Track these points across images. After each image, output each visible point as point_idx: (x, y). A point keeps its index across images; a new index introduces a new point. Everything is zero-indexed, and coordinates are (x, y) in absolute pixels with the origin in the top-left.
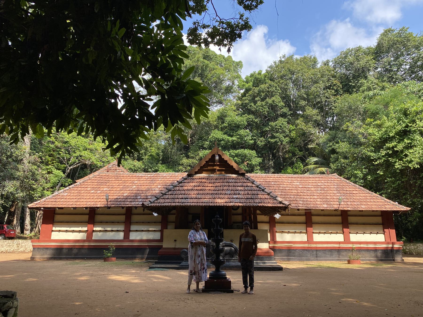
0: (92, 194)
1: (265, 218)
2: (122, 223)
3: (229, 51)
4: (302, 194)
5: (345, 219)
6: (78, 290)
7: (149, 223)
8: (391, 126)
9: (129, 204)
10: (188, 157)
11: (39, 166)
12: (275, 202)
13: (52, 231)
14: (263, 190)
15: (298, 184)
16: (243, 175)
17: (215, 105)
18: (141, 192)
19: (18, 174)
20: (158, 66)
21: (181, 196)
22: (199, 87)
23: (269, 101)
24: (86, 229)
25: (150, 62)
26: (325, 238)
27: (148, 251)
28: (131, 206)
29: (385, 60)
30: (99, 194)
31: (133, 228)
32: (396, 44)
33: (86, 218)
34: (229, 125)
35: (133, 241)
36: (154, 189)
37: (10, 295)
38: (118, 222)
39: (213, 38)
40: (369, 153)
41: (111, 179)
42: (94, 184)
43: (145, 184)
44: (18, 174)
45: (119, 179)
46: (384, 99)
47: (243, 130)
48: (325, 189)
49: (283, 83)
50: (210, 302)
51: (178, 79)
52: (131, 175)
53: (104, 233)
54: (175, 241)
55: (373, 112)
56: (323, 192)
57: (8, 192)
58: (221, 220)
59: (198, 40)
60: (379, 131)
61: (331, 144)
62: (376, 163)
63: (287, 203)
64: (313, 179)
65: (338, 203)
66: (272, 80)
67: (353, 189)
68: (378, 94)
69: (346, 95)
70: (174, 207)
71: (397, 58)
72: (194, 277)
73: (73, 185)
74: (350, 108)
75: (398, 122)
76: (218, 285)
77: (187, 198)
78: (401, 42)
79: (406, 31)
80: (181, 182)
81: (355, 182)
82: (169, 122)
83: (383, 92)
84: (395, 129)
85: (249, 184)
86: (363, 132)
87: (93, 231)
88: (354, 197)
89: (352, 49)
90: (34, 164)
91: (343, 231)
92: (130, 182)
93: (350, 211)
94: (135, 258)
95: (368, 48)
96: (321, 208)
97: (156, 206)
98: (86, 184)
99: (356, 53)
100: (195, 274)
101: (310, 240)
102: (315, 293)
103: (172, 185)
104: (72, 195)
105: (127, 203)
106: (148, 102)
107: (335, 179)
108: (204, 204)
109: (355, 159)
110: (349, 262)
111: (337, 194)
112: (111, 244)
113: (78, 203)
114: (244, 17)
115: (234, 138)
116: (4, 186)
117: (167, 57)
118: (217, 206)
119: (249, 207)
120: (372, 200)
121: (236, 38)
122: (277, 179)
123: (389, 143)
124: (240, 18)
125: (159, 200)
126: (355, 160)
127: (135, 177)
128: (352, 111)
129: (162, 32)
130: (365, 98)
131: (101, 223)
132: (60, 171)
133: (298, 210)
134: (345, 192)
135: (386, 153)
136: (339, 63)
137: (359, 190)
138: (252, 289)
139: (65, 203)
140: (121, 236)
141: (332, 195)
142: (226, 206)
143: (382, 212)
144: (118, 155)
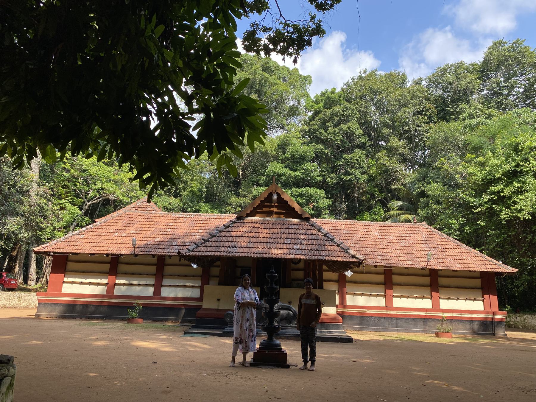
0: (116, 238)
1: (334, 276)
2: (152, 275)
3: (295, 61)
4: (380, 247)
5: (434, 281)
6: (93, 357)
7: (186, 276)
8: (497, 165)
9: (161, 252)
10: (238, 195)
11: (49, 200)
12: (347, 255)
13: (64, 282)
14: (332, 240)
15: (377, 234)
16: (307, 219)
17: (275, 129)
18: (177, 237)
19: (23, 208)
20: (204, 76)
21: (227, 244)
22: (255, 105)
24: (106, 281)
25: (194, 71)
26: (407, 303)
27: (183, 311)
28: (164, 254)
29: (493, 80)
30: (125, 238)
31: (165, 282)
32: (508, 61)
33: (107, 267)
34: (292, 156)
35: (165, 298)
36: (193, 234)
37: (5, 360)
38: (147, 275)
39: (275, 45)
40: (468, 198)
41: (140, 220)
42: (118, 224)
43: (182, 227)
44: (23, 208)
45: (150, 220)
46: (489, 130)
47: (309, 163)
48: (411, 242)
49: (362, 105)
50: (260, 379)
51: (227, 93)
52: (165, 216)
53: (129, 287)
54: (219, 300)
55: (475, 145)
56: (407, 245)
57: (9, 231)
58: (276, 276)
59: (257, 46)
60: (482, 170)
61: (420, 185)
62: (477, 211)
63: (361, 257)
64: (395, 228)
65: (426, 260)
66: (348, 100)
67: (446, 243)
68: (482, 124)
69: (442, 124)
70: (219, 258)
71: (508, 78)
72: (240, 346)
73: (91, 225)
74: (446, 139)
75: (506, 160)
76: (270, 358)
77: (236, 247)
78: (515, 59)
79: (521, 44)
80: (228, 227)
81: (449, 234)
82: (215, 149)
83: (489, 121)
84: (502, 168)
85: (315, 232)
86: (462, 170)
87: (116, 284)
88: (447, 253)
89: (452, 65)
90: (43, 197)
91: (431, 295)
92: (164, 224)
93: (441, 270)
94: (166, 320)
95: (472, 65)
96: (405, 266)
97: (195, 255)
98: (108, 224)
99: (456, 71)
100: (241, 342)
101: (389, 306)
102: (393, 372)
103: (217, 230)
104: (90, 237)
105: (160, 250)
106: (189, 122)
107: (424, 230)
108: (256, 255)
109: (450, 205)
110: (437, 335)
111: (426, 249)
112: (138, 301)
113: (98, 249)
114: (316, 19)
115: (298, 173)
116: (4, 224)
117: (215, 65)
118: (272, 258)
119: (313, 261)
120: (469, 258)
121: (304, 45)
122: (350, 226)
123: (494, 186)
124: (311, 21)
125: (199, 248)
126: (450, 206)
127: (170, 218)
128: (449, 145)
129: (210, 33)
130: (465, 128)
131: (125, 274)
132: (75, 207)
133: (376, 266)
134: (435, 246)
135: (489, 199)
136: (435, 81)
137: (454, 244)
138: (313, 364)
139: (80, 248)
140: (150, 291)
141: (418, 249)
142: (284, 259)
143: (482, 273)
144: (149, 187)
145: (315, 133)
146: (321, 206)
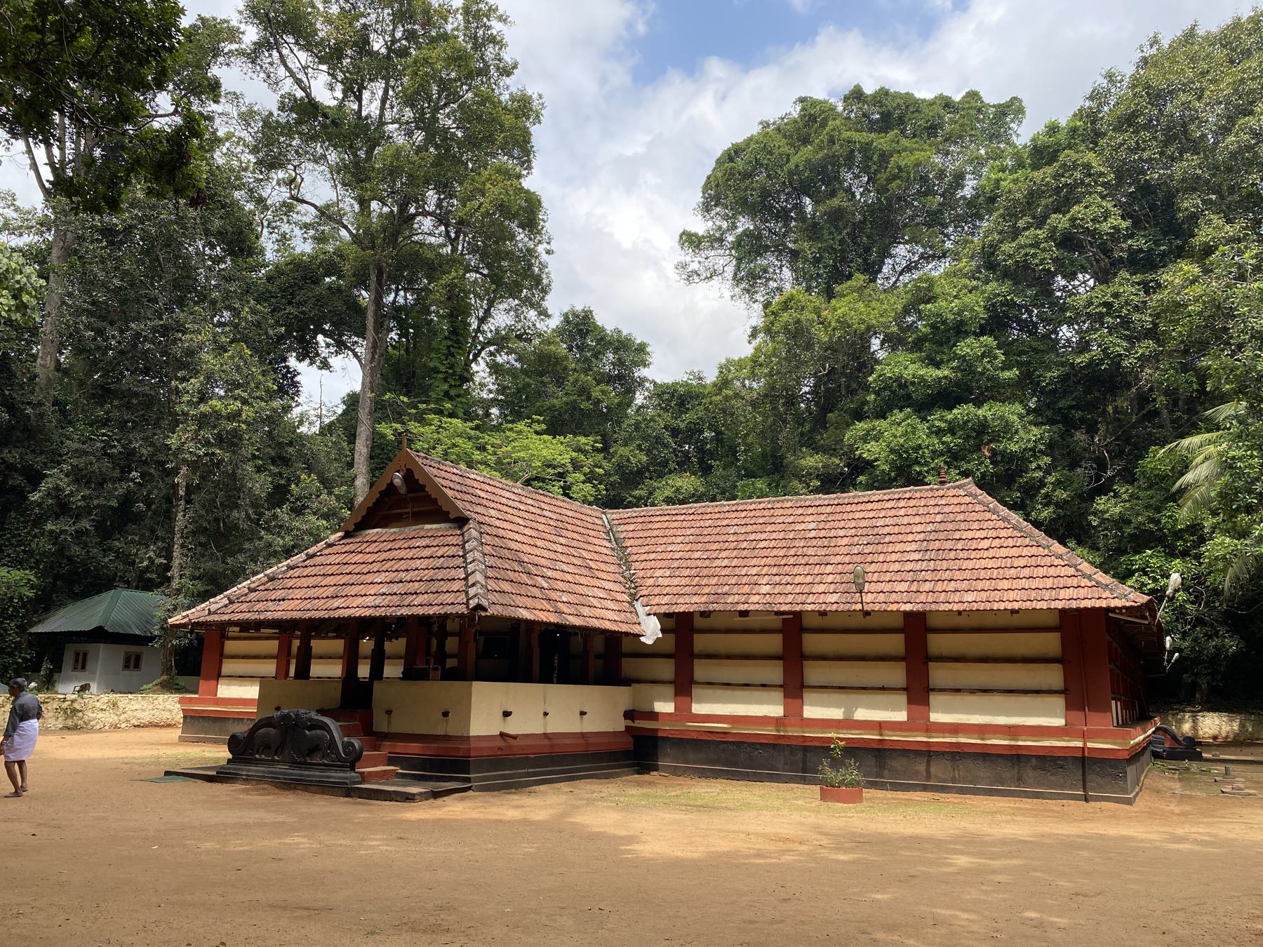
10: (817, 449)
23: (1060, 221)
49: (1121, 145)
70: (402, 620)
115: (939, 373)
133: (744, 614)
143: (1063, 612)
145: (993, 253)
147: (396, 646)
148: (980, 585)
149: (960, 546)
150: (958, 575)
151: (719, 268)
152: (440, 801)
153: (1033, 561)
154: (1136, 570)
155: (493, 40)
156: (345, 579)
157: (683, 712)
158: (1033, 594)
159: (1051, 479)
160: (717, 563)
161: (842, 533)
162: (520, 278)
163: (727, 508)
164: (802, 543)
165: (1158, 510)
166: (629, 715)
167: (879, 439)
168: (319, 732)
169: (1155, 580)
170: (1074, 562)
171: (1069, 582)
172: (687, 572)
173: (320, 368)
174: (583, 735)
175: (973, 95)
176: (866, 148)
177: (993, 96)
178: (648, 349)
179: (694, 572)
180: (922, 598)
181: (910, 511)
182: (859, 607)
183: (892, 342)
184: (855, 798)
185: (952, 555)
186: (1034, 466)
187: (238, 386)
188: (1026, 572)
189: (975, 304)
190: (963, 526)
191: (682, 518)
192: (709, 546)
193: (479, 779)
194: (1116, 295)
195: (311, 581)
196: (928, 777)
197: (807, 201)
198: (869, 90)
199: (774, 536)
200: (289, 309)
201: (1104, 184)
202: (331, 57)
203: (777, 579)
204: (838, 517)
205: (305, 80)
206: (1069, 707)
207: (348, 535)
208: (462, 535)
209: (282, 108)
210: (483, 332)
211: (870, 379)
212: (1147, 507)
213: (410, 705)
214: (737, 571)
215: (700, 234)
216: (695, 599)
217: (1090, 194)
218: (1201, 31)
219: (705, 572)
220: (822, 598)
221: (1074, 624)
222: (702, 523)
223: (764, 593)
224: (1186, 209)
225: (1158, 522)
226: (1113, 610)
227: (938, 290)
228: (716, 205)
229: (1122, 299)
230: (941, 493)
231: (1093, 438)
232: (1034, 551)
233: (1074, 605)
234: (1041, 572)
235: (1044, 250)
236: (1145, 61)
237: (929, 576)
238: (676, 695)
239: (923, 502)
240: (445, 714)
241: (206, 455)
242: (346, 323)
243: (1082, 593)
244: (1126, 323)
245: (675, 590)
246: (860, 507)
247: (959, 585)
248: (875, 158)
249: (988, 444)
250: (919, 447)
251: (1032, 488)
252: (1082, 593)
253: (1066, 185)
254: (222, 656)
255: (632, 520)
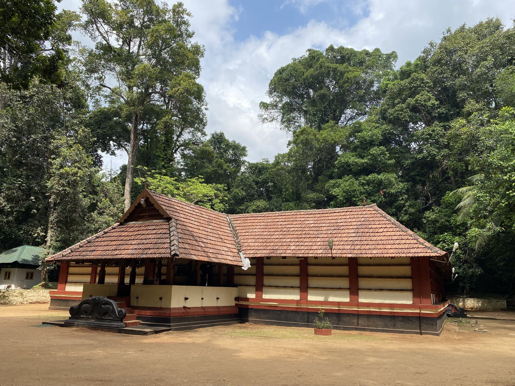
10: (314, 191)
23: (411, 101)
49: (435, 71)
70: (143, 259)
115: (363, 161)
133: (284, 258)
143: (412, 258)
145: (385, 113)
146: (393, 191)
147: (140, 270)
148: (379, 247)
149: (371, 231)
150: (370, 243)
151: (275, 117)
152: (158, 335)
153: (400, 237)
154: (441, 241)
155: (184, 23)
156: (120, 242)
157: (259, 298)
158: (400, 251)
159: (407, 204)
160: (273, 237)
161: (324, 225)
162: (194, 119)
163: (278, 215)
164: (308, 229)
165: (450, 217)
166: (237, 299)
167: (340, 187)
168: (108, 306)
169: (448, 245)
170: (416, 238)
171: (415, 246)
172: (261, 240)
173: (111, 155)
174: (218, 307)
175: (377, 50)
176: (335, 70)
177: (385, 51)
178: (247, 149)
179: (264, 240)
180: (356, 252)
181: (351, 217)
182: (330, 255)
183: (344, 148)
184: (329, 333)
185: (368, 234)
186: (401, 198)
187: (77, 162)
188: (397, 242)
189: (378, 133)
190: (372, 223)
191: (260, 218)
192: (270, 230)
193: (174, 326)
194: (433, 131)
195: (105, 243)
196: (358, 325)
197: (311, 91)
198: (336, 47)
199: (297, 226)
200: (98, 130)
201: (429, 87)
202: (118, 27)
203: (298, 243)
204: (323, 218)
205: (107, 37)
206: (414, 296)
207: (121, 224)
208: (169, 224)
209: (97, 48)
210: (179, 141)
211: (336, 163)
212: (445, 216)
213: (146, 295)
214: (282, 240)
215: (268, 103)
216: (264, 251)
217: (423, 90)
218: (467, 27)
219: (269, 240)
220: (316, 252)
221: (417, 264)
222: (267, 220)
223: (293, 249)
224: (461, 97)
225: (449, 222)
226: (430, 257)
227: (363, 127)
228: (274, 92)
229: (436, 132)
230: (364, 209)
231: (424, 188)
232: (401, 233)
233: (416, 255)
234: (403, 241)
235: (405, 112)
236: (445, 38)
237: (358, 243)
238: (256, 291)
239: (356, 213)
240: (161, 299)
241: (62, 190)
242: (122, 136)
243: (419, 250)
244: (437, 142)
245: (256, 248)
246: (331, 215)
247: (370, 247)
248: (338, 74)
249: (382, 189)
250: (355, 190)
251: (400, 207)
252: (419, 250)
253: (414, 87)
254: (68, 274)
255: (239, 219)
